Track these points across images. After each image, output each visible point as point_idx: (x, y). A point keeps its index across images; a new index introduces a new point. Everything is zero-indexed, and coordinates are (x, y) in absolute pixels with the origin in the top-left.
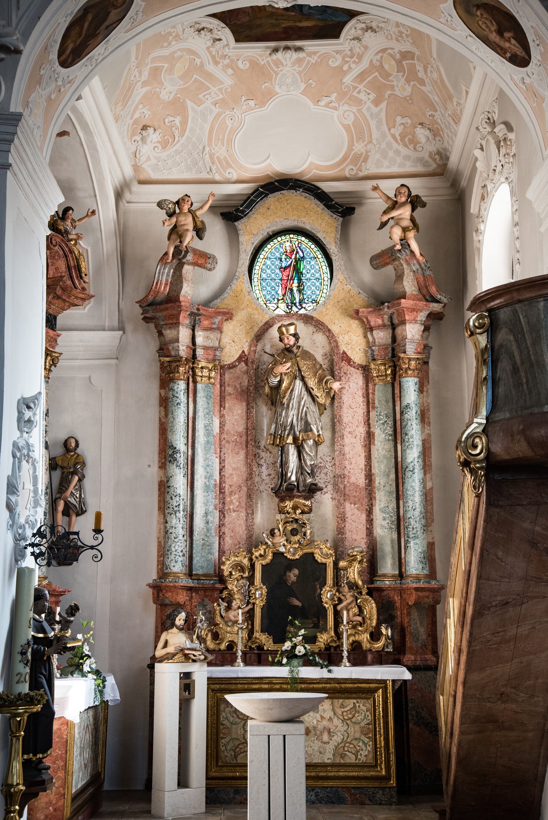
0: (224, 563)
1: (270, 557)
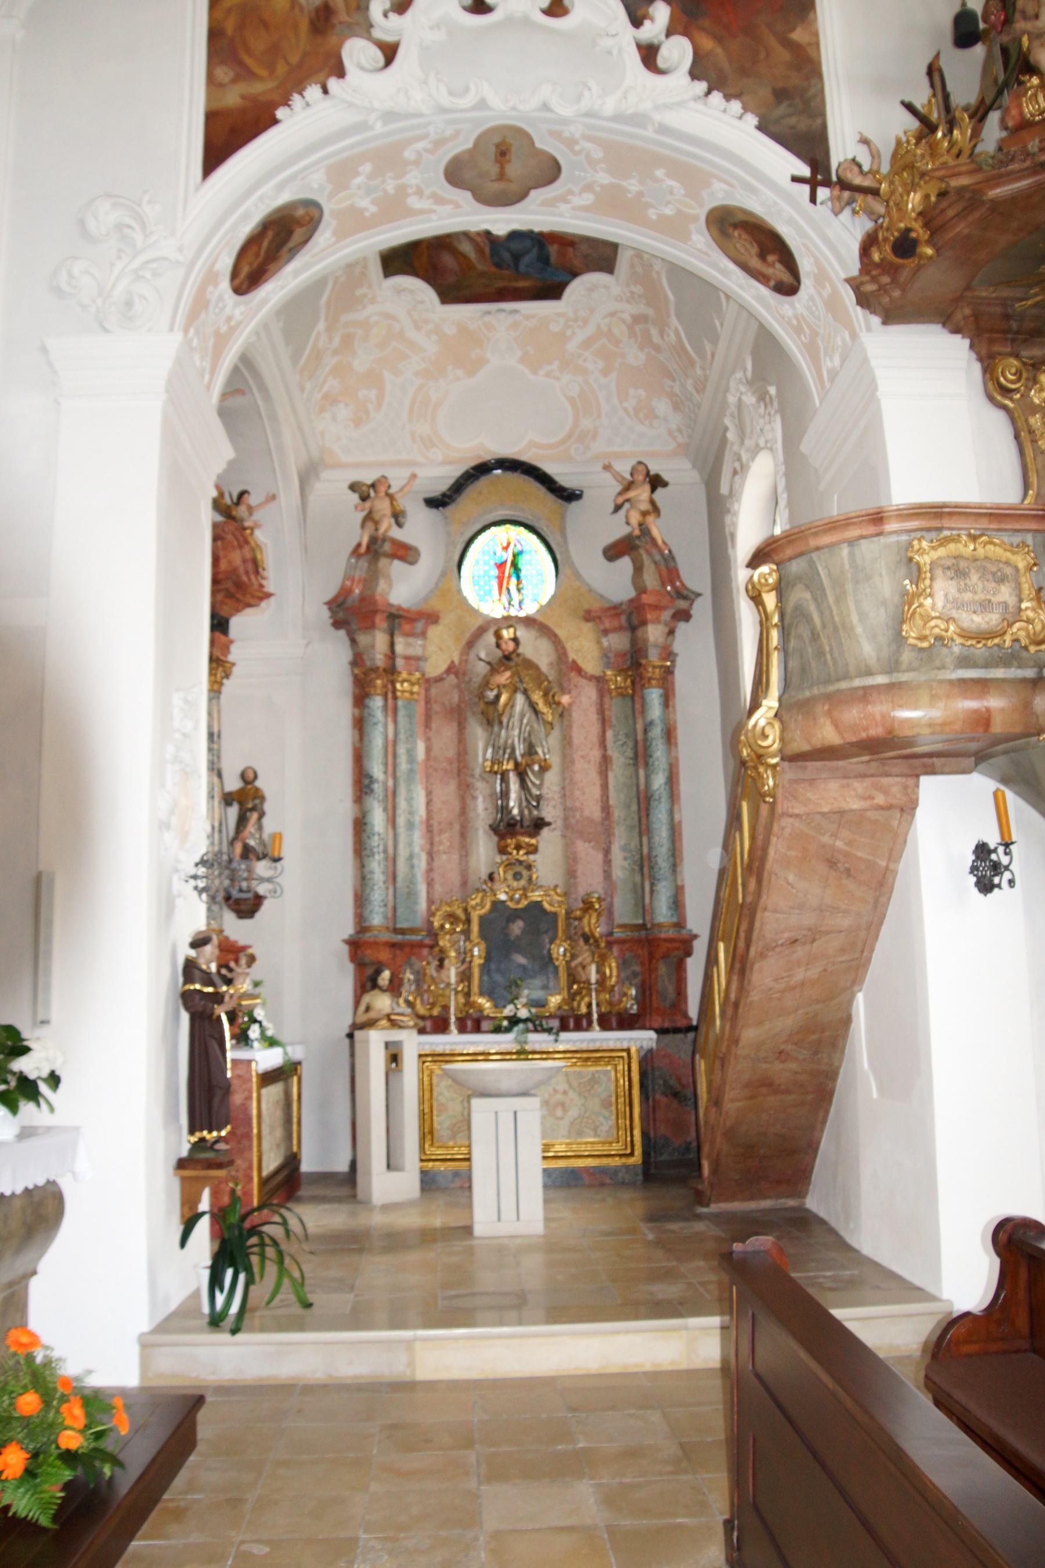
0: (433, 914)
1: (488, 906)
